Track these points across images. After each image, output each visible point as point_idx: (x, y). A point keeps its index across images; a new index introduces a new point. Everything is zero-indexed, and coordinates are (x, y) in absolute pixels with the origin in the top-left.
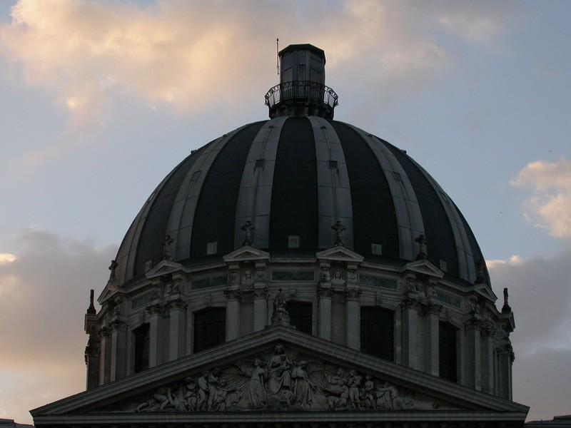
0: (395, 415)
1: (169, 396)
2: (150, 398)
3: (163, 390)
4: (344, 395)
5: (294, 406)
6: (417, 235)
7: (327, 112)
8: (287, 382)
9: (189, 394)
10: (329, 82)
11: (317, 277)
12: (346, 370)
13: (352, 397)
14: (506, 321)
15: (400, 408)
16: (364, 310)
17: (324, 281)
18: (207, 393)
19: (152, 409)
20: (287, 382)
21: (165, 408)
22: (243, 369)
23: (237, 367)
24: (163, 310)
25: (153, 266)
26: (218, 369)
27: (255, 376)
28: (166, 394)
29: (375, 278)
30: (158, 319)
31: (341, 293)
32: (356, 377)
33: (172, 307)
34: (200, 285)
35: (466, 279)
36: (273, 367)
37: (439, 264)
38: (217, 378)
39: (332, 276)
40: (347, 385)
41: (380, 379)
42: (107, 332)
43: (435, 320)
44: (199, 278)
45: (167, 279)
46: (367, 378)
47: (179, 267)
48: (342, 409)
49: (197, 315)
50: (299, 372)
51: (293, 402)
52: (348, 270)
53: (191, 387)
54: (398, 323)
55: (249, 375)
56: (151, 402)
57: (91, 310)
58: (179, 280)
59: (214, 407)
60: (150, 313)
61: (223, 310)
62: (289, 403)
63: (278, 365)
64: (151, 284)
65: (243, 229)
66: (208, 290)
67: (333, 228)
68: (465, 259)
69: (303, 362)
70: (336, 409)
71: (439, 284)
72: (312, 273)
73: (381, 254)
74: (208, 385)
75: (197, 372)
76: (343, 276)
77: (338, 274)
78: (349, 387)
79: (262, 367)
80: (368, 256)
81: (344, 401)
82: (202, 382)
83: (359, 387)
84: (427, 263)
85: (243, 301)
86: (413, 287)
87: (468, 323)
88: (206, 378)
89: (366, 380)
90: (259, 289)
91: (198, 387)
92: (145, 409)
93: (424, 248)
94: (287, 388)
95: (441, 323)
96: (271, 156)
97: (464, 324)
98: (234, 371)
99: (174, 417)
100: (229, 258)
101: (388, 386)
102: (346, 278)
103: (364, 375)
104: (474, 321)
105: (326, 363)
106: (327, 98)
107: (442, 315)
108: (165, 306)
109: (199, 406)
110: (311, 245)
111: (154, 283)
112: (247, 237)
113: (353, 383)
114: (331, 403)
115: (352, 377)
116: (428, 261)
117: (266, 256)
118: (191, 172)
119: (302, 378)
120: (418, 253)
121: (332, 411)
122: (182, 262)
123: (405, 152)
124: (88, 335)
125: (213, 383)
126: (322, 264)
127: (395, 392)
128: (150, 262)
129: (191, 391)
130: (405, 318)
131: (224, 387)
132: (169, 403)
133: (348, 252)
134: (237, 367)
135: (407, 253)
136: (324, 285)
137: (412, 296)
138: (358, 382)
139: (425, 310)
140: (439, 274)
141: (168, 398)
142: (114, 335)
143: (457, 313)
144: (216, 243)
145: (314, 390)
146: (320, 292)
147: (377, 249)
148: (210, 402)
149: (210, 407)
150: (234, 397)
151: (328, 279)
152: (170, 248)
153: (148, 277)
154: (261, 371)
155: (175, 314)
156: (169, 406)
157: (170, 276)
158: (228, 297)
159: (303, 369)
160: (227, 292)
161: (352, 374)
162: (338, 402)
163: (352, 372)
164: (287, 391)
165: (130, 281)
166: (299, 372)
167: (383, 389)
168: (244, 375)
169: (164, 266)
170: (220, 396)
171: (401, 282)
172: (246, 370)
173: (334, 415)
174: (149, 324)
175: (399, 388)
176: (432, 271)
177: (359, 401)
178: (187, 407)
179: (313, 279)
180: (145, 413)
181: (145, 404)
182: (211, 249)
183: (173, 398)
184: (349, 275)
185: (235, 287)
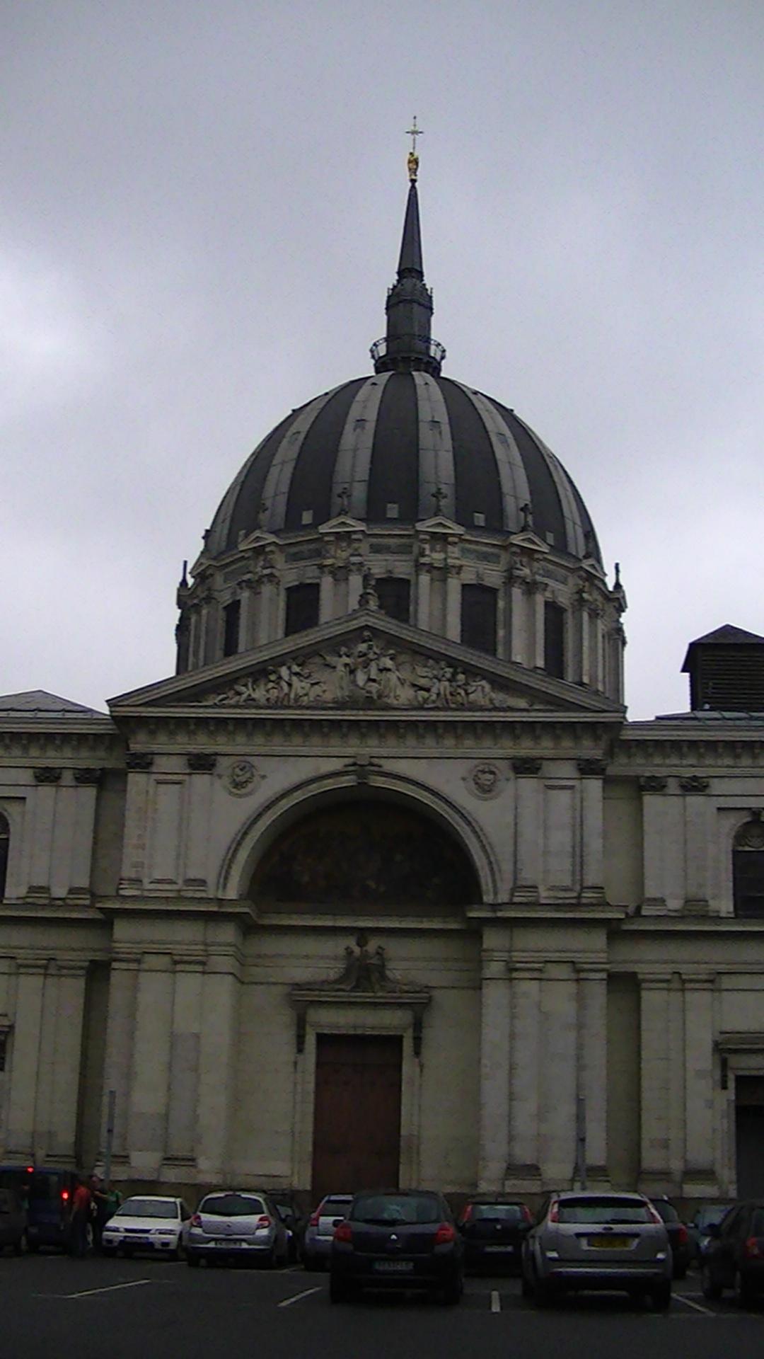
0: (486, 713)
1: (250, 685)
2: (230, 689)
3: (243, 681)
4: (434, 690)
5: (379, 701)
6: (522, 505)
7: (433, 367)
8: (374, 673)
9: (271, 685)
10: (435, 335)
11: (415, 550)
12: (437, 661)
13: (442, 692)
14: (616, 601)
15: (491, 706)
17: (423, 555)
18: (290, 685)
19: (232, 702)
20: (374, 673)
21: (245, 701)
22: (328, 658)
23: (321, 656)
24: (254, 586)
25: (247, 536)
26: (301, 657)
27: (340, 668)
28: (245, 685)
29: (475, 551)
30: (249, 598)
31: (439, 569)
32: (447, 669)
33: (263, 582)
34: (295, 558)
35: (574, 553)
36: (360, 657)
37: (545, 536)
38: (300, 668)
39: (432, 550)
40: (437, 678)
41: (473, 672)
42: (197, 608)
43: (540, 599)
44: (293, 550)
45: (259, 551)
46: (459, 670)
47: (272, 538)
48: (431, 706)
49: (288, 589)
50: (388, 663)
51: (380, 697)
52: (450, 544)
53: (273, 677)
54: (501, 604)
55: (334, 665)
56: (231, 694)
57: (184, 582)
58: (272, 552)
59: (296, 700)
60: (241, 588)
61: (317, 587)
62: (375, 697)
63: (365, 655)
64: (243, 557)
65: (340, 496)
66: (302, 563)
67: (433, 495)
69: (391, 652)
70: (426, 706)
71: (545, 559)
72: (411, 546)
73: (482, 524)
74: (290, 677)
75: (279, 661)
76: (444, 551)
77: (438, 547)
78: (440, 680)
79: (348, 656)
80: (470, 525)
81: (434, 697)
82: (284, 672)
83: (449, 680)
84: (531, 535)
85: (337, 577)
86: (516, 563)
87: (576, 603)
88: (289, 668)
89: (458, 673)
90: (354, 564)
91: (280, 678)
92: (224, 702)
93: (530, 518)
94: (374, 681)
95: (547, 604)
96: (372, 415)
97: (572, 604)
98: (317, 660)
99: (254, 711)
100: (323, 529)
101: (480, 681)
102: (446, 552)
103: (455, 668)
104: (581, 601)
105: (416, 653)
106: (433, 351)
107: (548, 594)
108: (257, 581)
109: (280, 700)
110: (411, 514)
111: (246, 556)
112: (343, 504)
113: (443, 676)
114: (420, 699)
115: (443, 669)
116: (533, 534)
117: (361, 527)
118: (289, 433)
119: (389, 670)
120: (522, 525)
121: (421, 708)
122: (275, 533)
123: (512, 410)
124: (179, 611)
125: (297, 674)
126: (422, 537)
127: (487, 687)
128: (244, 531)
129: (273, 682)
130: (509, 597)
131: (306, 678)
132: (250, 695)
133: (449, 523)
134: (321, 656)
135: (512, 526)
136: (423, 560)
137: (517, 573)
138: (448, 675)
139: (531, 588)
140: (545, 549)
141: (248, 689)
142: (204, 612)
144: (311, 511)
145: (402, 684)
146: (418, 567)
147: (480, 519)
148: (292, 696)
149: (292, 701)
150: (317, 689)
151: (427, 552)
152: (263, 517)
153: (241, 549)
154: (347, 660)
155: (267, 590)
156: (250, 699)
157: (263, 546)
158: (323, 572)
159: (391, 659)
160: (321, 567)
161: (443, 666)
162: (428, 698)
163: (443, 664)
164: (375, 685)
165: (222, 553)
166: (388, 663)
167: (475, 684)
168: (327, 665)
169: (258, 537)
170: (303, 688)
171: (505, 558)
172: (331, 659)
173: (424, 713)
174: (239, 601)
175: (492, 683)
176: (538, 545)
177: (449, 697)
178: (268, 700)
179: (411, 553)
180: (224, 706)
181: (225, 696)
182: (307, 518)
183: (254, 690)
184: (450, 548)
185: (329, 562)
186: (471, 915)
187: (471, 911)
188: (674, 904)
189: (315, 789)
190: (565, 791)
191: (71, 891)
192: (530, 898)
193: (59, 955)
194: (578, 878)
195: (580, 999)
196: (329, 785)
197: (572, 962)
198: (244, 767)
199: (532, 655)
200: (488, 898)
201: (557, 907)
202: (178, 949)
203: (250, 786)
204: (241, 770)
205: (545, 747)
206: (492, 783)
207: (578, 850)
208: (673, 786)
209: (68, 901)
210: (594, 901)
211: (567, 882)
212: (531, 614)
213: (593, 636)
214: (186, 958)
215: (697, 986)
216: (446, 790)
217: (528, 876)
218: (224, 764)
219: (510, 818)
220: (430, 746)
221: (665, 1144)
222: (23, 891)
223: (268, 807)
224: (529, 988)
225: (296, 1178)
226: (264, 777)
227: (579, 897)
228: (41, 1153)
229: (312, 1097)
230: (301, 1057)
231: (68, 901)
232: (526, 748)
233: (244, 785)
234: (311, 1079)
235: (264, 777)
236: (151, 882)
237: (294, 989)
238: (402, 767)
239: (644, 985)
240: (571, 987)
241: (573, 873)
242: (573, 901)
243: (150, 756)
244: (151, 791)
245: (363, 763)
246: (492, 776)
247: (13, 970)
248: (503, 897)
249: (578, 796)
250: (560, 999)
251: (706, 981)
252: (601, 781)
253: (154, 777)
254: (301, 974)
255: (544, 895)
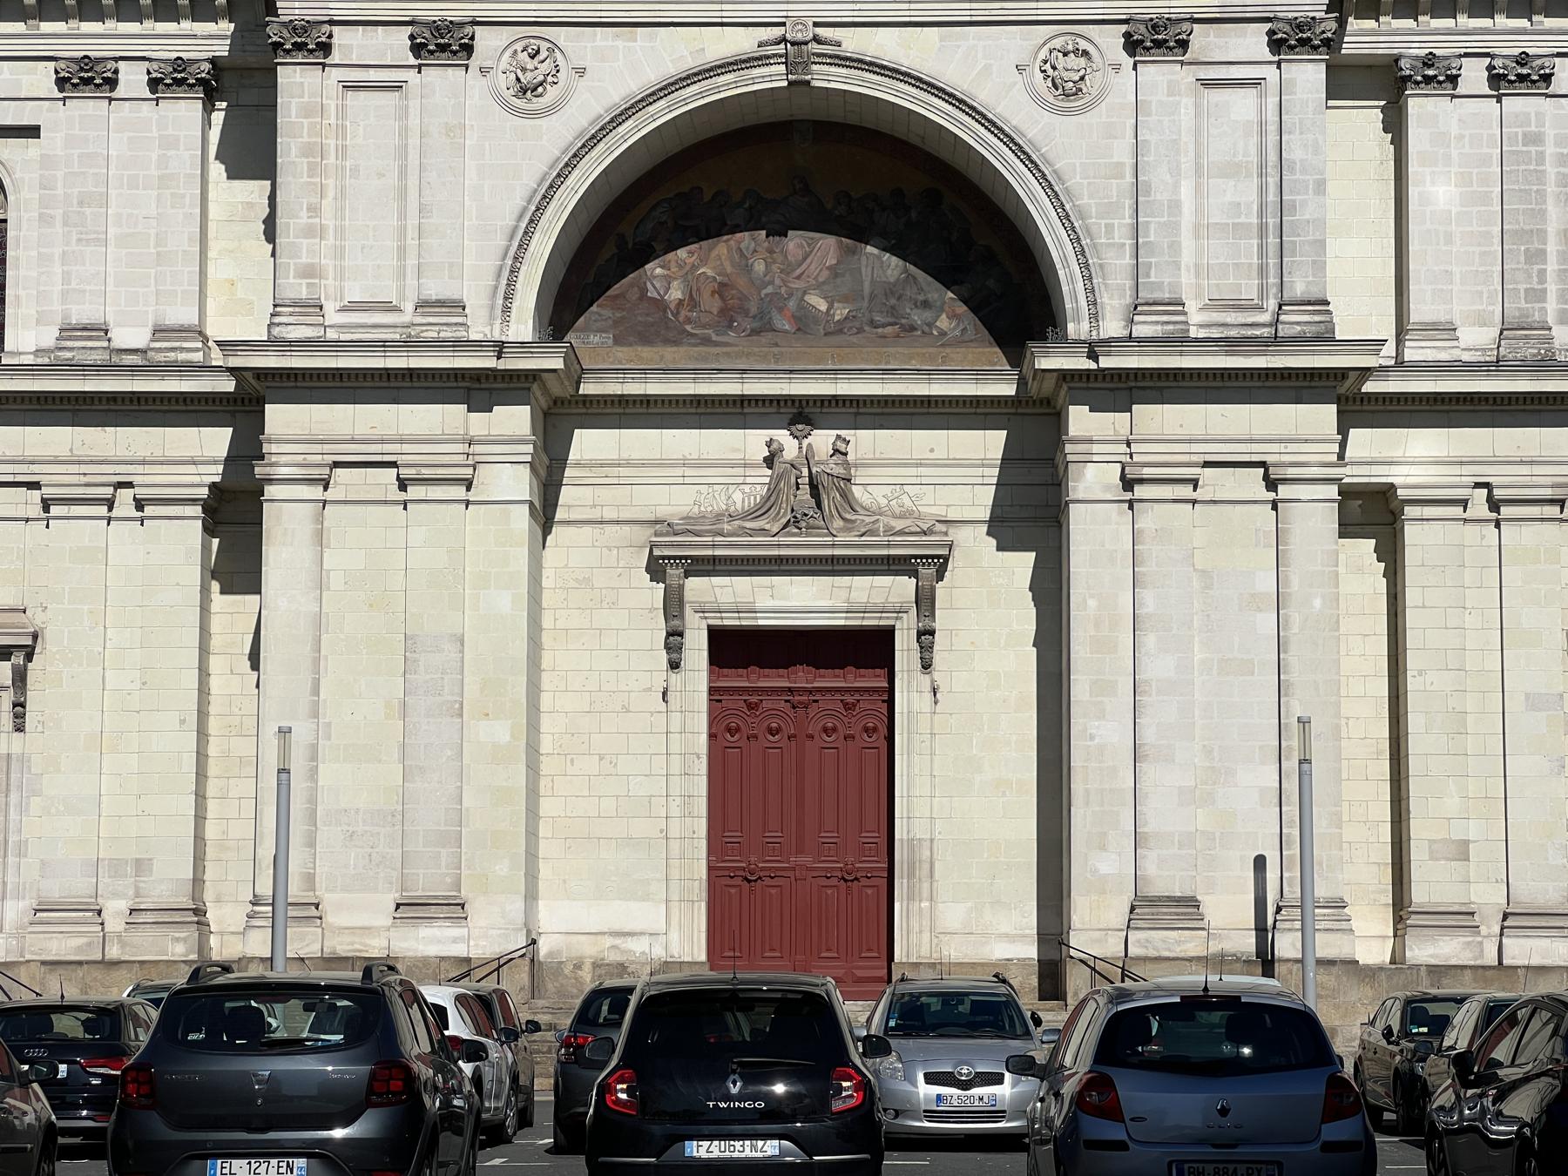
186: (1044, 363)
187: (1046, 355)
188: (1476, 339)
189: (694, 98)
190: (1241, 92)
191: (159, 331)
192: (1171, 327)
193: (138, 475)
194: (1273, 280)
196: (727, 87)
197: (1263, 464)
198: (538, 52)
200: (1077, 328)
201: (1231, 344)
202: (408, 454)
203: (551, 93)
204: (532, 57)
206: (1082, 78)
207: (1272, 221)
208: (1474, 75)
209: (160, 357)
210: (1310, 331)
211: (1250, 291)
214: (427, 472)
215: (1534, 511)
216: (982, 97)
217: (1159, 281)
218: (486, 41)
219: (1122, 152)
221: (1462, 851)
222: (49, 337)
223: (594, 140)
225: (674, 936)
226: (581, 72)
227: (1276, 322)
228: (115, 909)
229: (702, 766)
230: (675, 678)
231: (150, 354)
233: (540, 89)
234: (701, 723)
235: (581, 72)
236: (343, 310)
237: (656, 535)
239: (1410, 511)
241: (1262, 271)
242: (1266, 332)
243: (326, 28)
244: (331, 105)
245: (799, 37)
246: (1082, 61)
247: (36, 510)
248: (1112, 327)
249: (1272, 101)
251: (1552, 502)
252: (1323, 66)
253: (335, 74)
254: (676, 501)
255: (1197, 320)
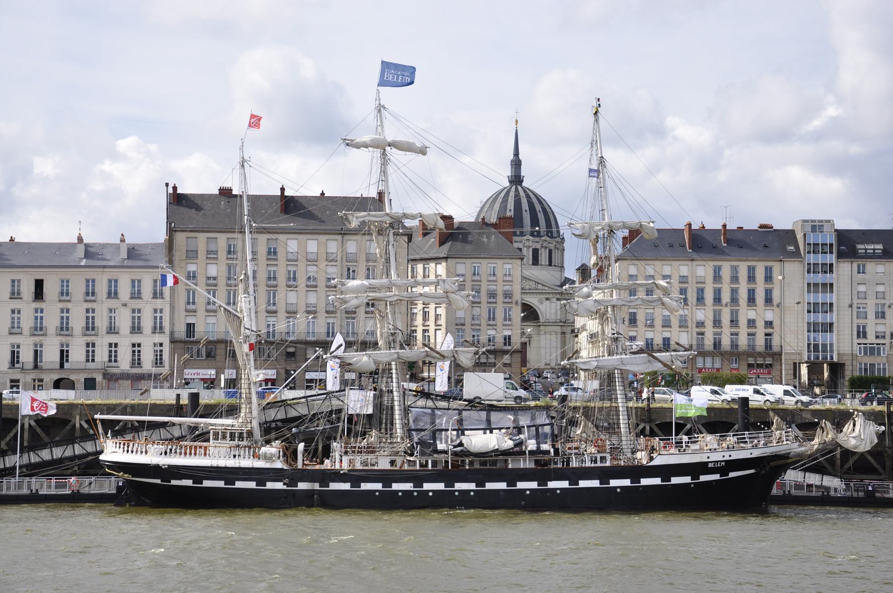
16: (533, 249)
43: (547, 250)
54: (540, 252)
68: (554, 230)
104: (556, 248)
121: (530, 289)
130: (541, 251)
139: (546, 248)
143: (552, 246)
166: (524, 281)
195: (557, 338)
199: (546, 262)
200: (541, 321)
205: (551, 296)
212: (546, 251)
213: (558, 254)
217: (548, 317)
220: (532, 296)
224: (548, 336)
232: (548, 296)
238: (527, 299)
240: (555, 336)
250: (553, 337)
